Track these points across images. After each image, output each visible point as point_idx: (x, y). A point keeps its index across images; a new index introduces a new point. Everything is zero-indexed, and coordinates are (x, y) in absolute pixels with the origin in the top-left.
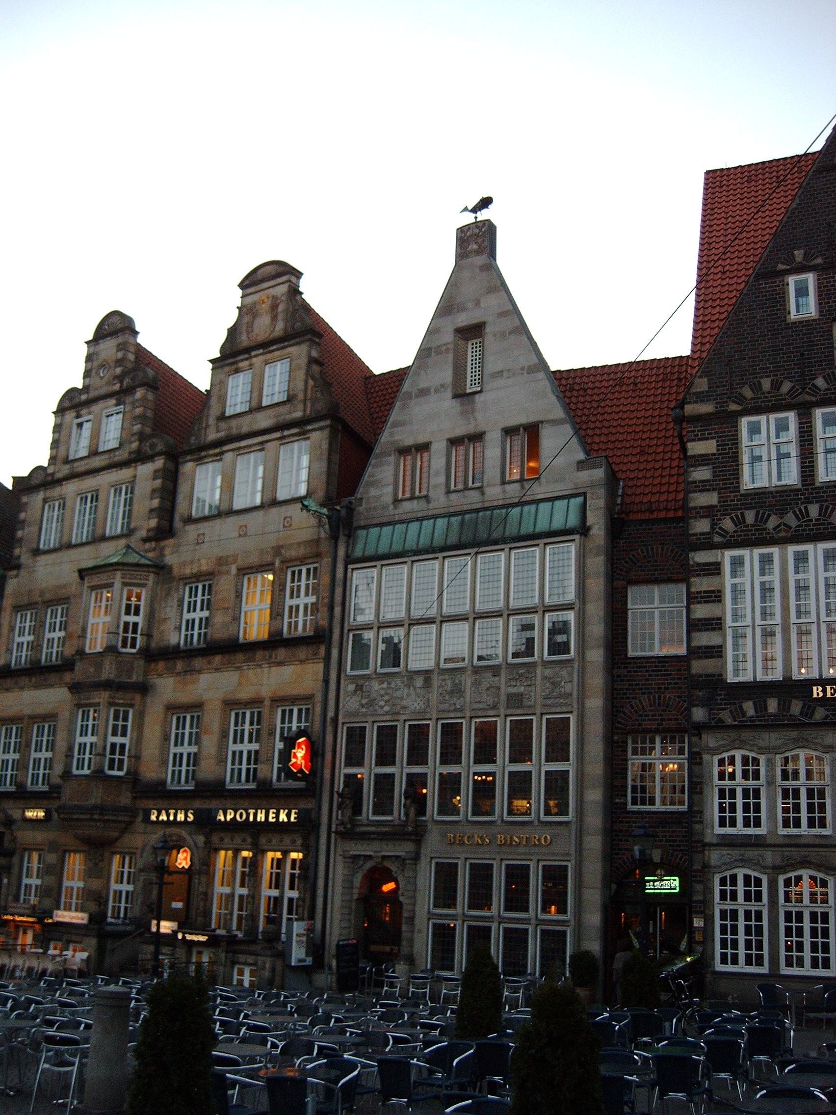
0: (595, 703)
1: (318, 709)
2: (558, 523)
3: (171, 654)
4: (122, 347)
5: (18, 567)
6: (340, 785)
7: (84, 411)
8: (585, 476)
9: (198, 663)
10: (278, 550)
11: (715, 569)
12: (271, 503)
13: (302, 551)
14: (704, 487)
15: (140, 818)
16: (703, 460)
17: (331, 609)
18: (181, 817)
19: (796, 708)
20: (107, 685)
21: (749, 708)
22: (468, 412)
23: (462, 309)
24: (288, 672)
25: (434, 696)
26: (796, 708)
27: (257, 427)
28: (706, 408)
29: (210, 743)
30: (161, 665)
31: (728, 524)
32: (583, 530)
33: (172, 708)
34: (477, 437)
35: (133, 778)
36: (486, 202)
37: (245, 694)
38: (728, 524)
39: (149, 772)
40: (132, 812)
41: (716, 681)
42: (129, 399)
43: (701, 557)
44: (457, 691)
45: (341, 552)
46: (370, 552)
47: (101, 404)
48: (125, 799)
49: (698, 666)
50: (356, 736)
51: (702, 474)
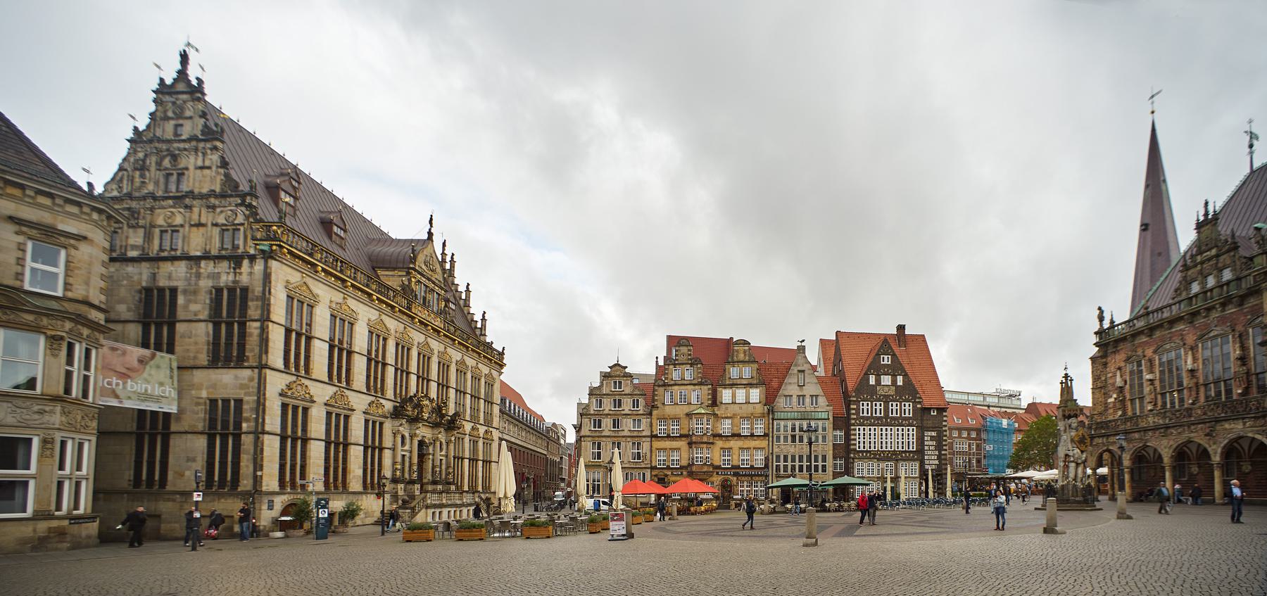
0: (831, 452)
1: (767, 451)
2: (823, 417)
3: (720, 436)
4: (689, 350)
5: (658, 407)
6: (775, 466)
7: (677, 366)
8: (828, 408)
9: (730, 438)
10: (752, 414)
11: (855, 430)
12: (748, 403)
13: (759, 415)
14: (853, 414)
15: (715, 473)
16: (854, 409)
17: (769, 429)
18: (729, 473)
19: (868, 455)
20: (705, 443)
21: (861, 455)
22: (802, 390)
23: (799, 366)
24: (757, 442)
25: (797, 450)
26: (868, 455)
27: (742, 383)
28: (855, 399)
29: (735, 457)
30: (717, 438)
31: (858, 422)
32: (829, 419)
33: (721, 448)
34: (804, 396)
35: (712, 465)
36: (803, 341)
37: (745, 446)
38: (858, 422)
39: (716, 463)
40: (713, 472)
41: (855, 450)
42: (695, 366)
43: (852, 427)
44: (802, 449)
45: (771, 417)
46: (779, 418)
47: (684, 366)
48: (711, 470)
49: (852, 447)
50: (778, 457)
51: (854, 412)
